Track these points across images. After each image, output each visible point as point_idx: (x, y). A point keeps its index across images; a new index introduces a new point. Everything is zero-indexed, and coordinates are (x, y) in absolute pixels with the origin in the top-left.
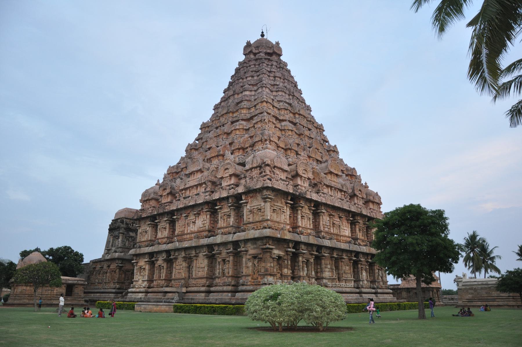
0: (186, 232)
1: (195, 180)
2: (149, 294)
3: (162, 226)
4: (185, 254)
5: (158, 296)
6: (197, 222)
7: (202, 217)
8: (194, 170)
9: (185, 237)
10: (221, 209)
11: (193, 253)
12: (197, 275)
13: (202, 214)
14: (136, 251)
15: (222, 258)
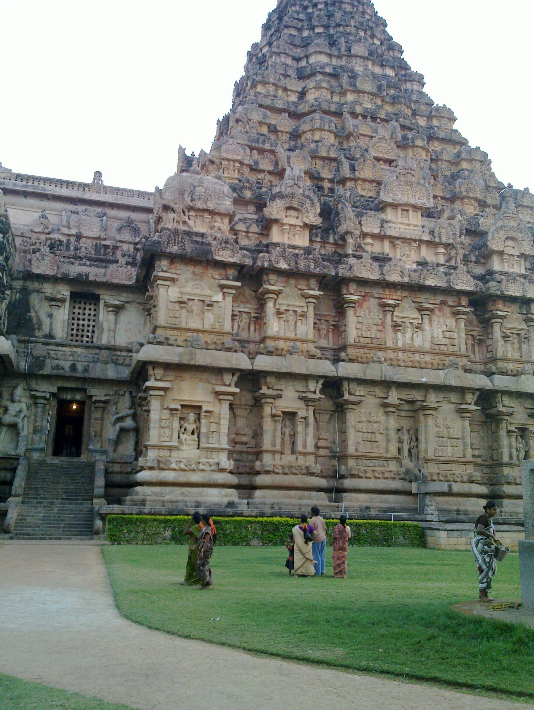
0: (390, 344)
1: (411, 227)
2: (258, 493)
3: (289, 305)
4: (398, 399)
5: (310, 498)
6: (426, 327)
7: (442, 320)
8: (412, 201)
9: (390, 354)
10: (502, 319)
11: (432, 399)
12: (441, 454)
13: (436, 311)
14: (192, 355)
15: (519, 424)
